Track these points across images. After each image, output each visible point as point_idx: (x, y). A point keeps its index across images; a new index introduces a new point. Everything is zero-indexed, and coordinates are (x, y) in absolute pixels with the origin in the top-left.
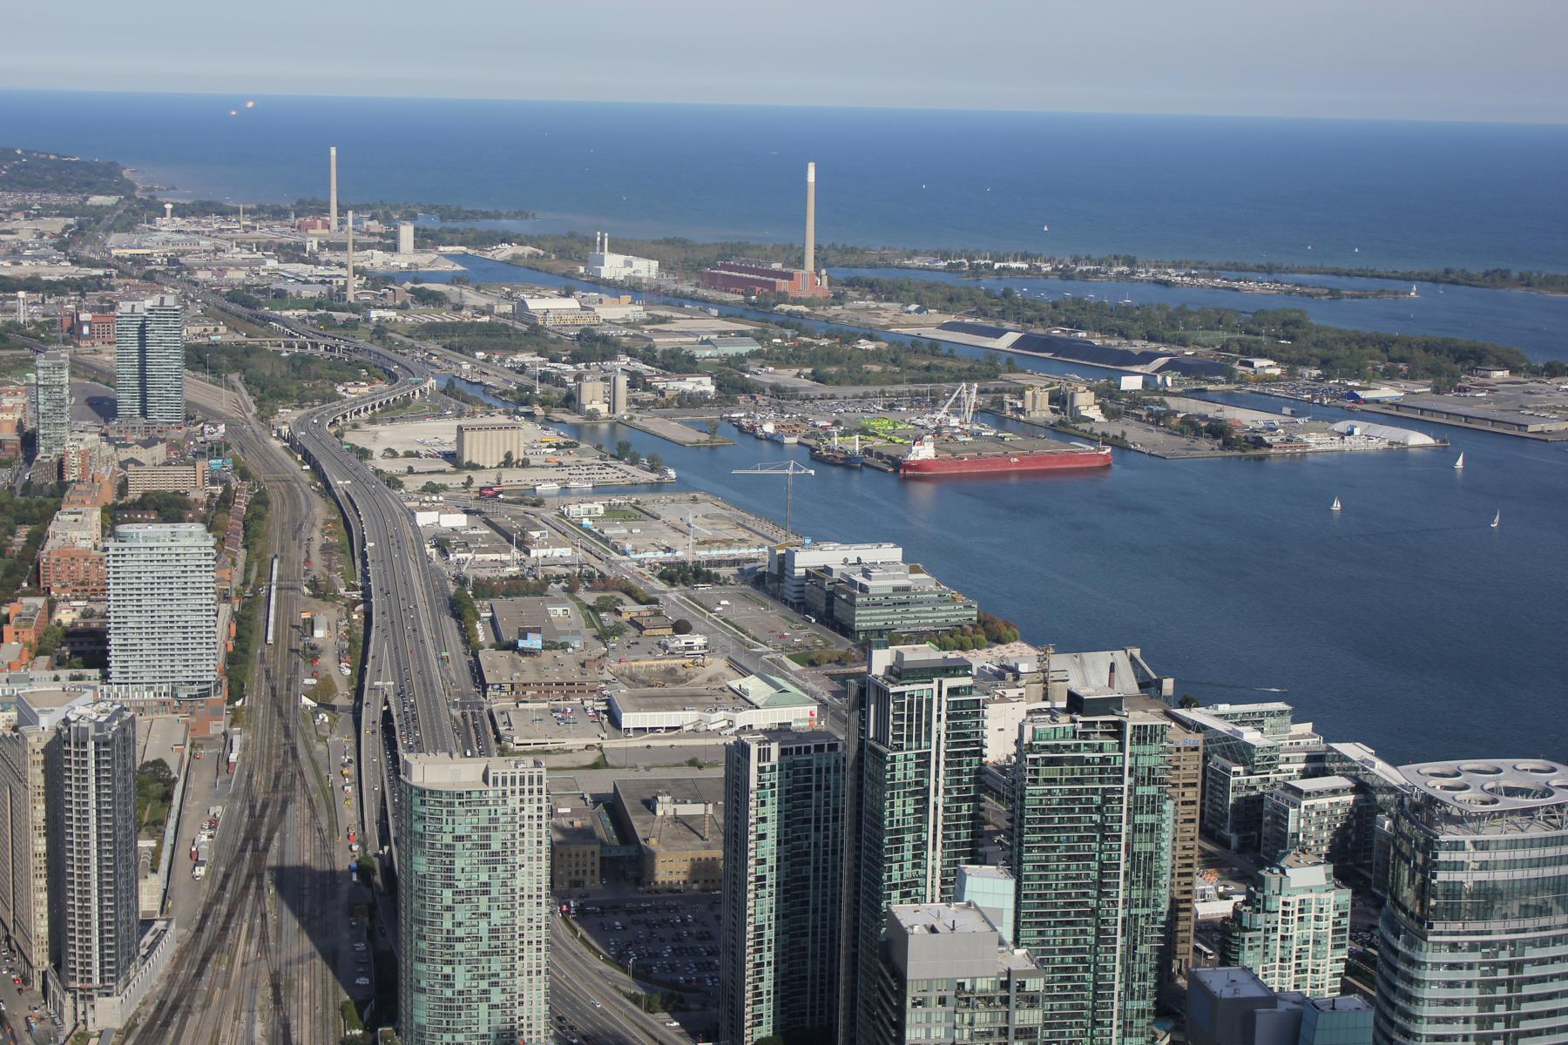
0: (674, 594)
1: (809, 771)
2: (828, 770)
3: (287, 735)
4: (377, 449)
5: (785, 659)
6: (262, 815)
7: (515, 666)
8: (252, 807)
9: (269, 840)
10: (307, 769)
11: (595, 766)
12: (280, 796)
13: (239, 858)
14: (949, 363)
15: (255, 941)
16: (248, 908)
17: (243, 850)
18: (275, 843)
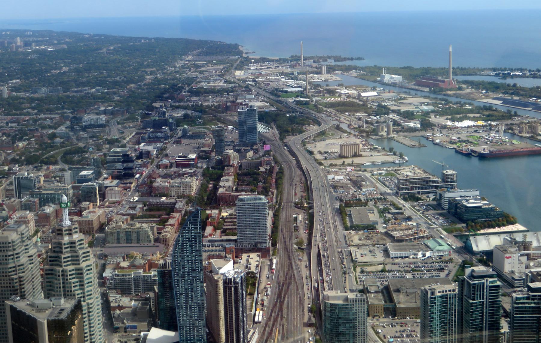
0: (407, 205)
1: (447, 298)
2: (453, 298)
3: (289, 259)
4: (316, 151)
5: (440, 229)
6: (282, 289)
8: (279, 286)
9: (284, 298)
10: (295, 272)
11: (383, 271)
12: (287, 282)
14: (496, 113)
15: (280, 335)
17: (277, 302)
18: (286, 299)
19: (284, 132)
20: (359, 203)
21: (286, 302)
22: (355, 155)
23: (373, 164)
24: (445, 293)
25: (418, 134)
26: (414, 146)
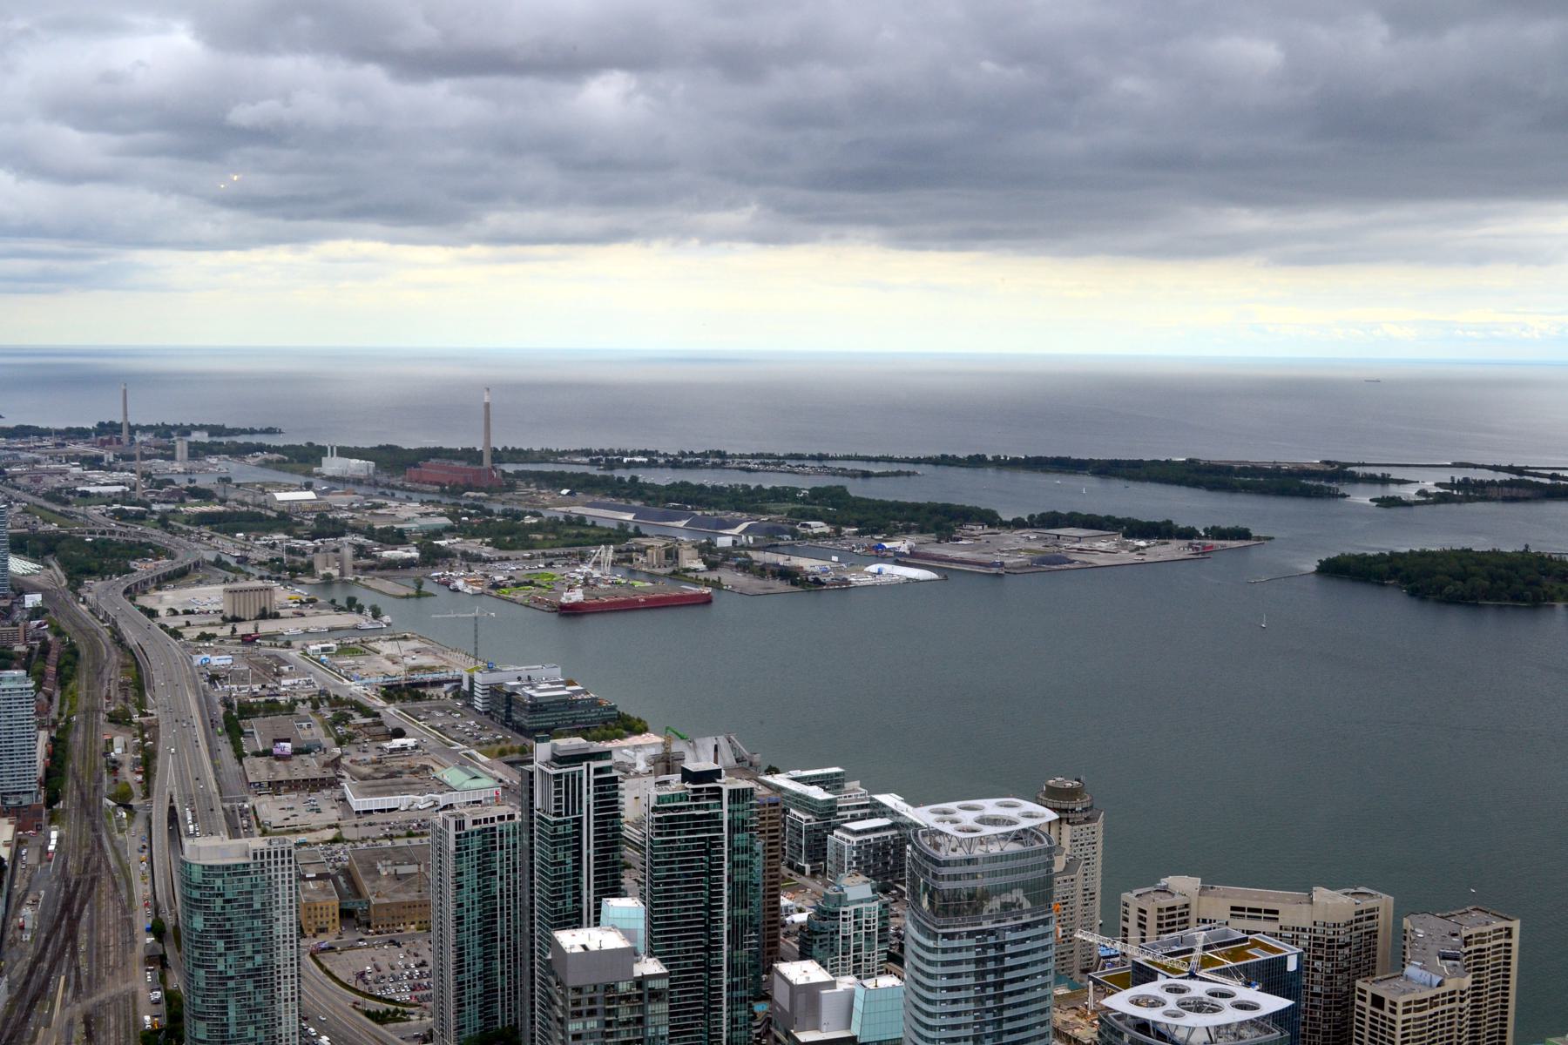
0: (392, 709)
3: (94, 830)
4: (163, 612)
5: (474, 752)
6: (75, 892)
7: (270, 767)
8: (67, 886)
9: (81, 911)
10: (110, 854)
11: (335, 841)
12: (88, 877)
13: (57, 926)
14: (592, 531)
15: (70, 990)
16: (65, 964)
17: (61, 919)
18: (86, 913)
19: (78, 573)
20: (272, 708)
21: (84, 919)
22: (264, 615)
23: (306, 632)
24: (490, 825)
25: (416, 572)
26: (408, 597)
